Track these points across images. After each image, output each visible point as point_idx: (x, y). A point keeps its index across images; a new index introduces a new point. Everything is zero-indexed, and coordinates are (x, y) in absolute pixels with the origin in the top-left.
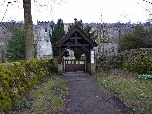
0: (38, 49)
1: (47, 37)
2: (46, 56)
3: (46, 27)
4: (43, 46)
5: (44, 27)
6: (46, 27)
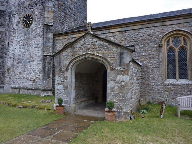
2: (20, 89)
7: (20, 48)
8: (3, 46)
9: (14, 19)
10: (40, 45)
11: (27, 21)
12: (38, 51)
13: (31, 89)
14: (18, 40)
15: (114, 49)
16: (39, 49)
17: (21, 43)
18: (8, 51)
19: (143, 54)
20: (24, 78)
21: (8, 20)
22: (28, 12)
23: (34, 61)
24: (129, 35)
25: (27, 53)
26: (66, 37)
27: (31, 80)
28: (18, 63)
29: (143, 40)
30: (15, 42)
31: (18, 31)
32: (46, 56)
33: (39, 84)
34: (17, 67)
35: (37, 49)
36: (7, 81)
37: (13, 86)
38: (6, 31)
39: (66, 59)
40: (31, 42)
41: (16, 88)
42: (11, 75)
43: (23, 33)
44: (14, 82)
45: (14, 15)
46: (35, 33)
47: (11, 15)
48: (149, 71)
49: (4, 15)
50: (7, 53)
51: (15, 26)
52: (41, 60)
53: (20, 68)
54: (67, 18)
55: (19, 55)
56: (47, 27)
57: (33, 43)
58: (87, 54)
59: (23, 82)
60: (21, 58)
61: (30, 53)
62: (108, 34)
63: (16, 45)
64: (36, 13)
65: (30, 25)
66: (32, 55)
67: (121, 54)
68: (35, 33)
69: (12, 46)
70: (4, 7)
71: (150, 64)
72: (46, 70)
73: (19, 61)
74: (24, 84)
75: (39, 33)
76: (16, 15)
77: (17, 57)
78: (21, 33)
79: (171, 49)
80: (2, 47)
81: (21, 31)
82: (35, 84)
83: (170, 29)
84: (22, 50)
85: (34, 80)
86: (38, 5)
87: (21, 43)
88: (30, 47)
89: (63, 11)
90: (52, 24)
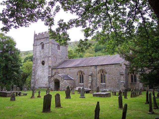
0: (33, 77)
1: (43, 57)
3: (42, 41)
5: (41, 42)
11: (43, 63)
13: (45, 87)
22: (44, 60)
26: (55, 70)
37: (39, 86)
39: (52, 79)
41: (40, 87)
43: (42, 67)
55: (41, 75)
56: (49, 67)
90: (51, 65)
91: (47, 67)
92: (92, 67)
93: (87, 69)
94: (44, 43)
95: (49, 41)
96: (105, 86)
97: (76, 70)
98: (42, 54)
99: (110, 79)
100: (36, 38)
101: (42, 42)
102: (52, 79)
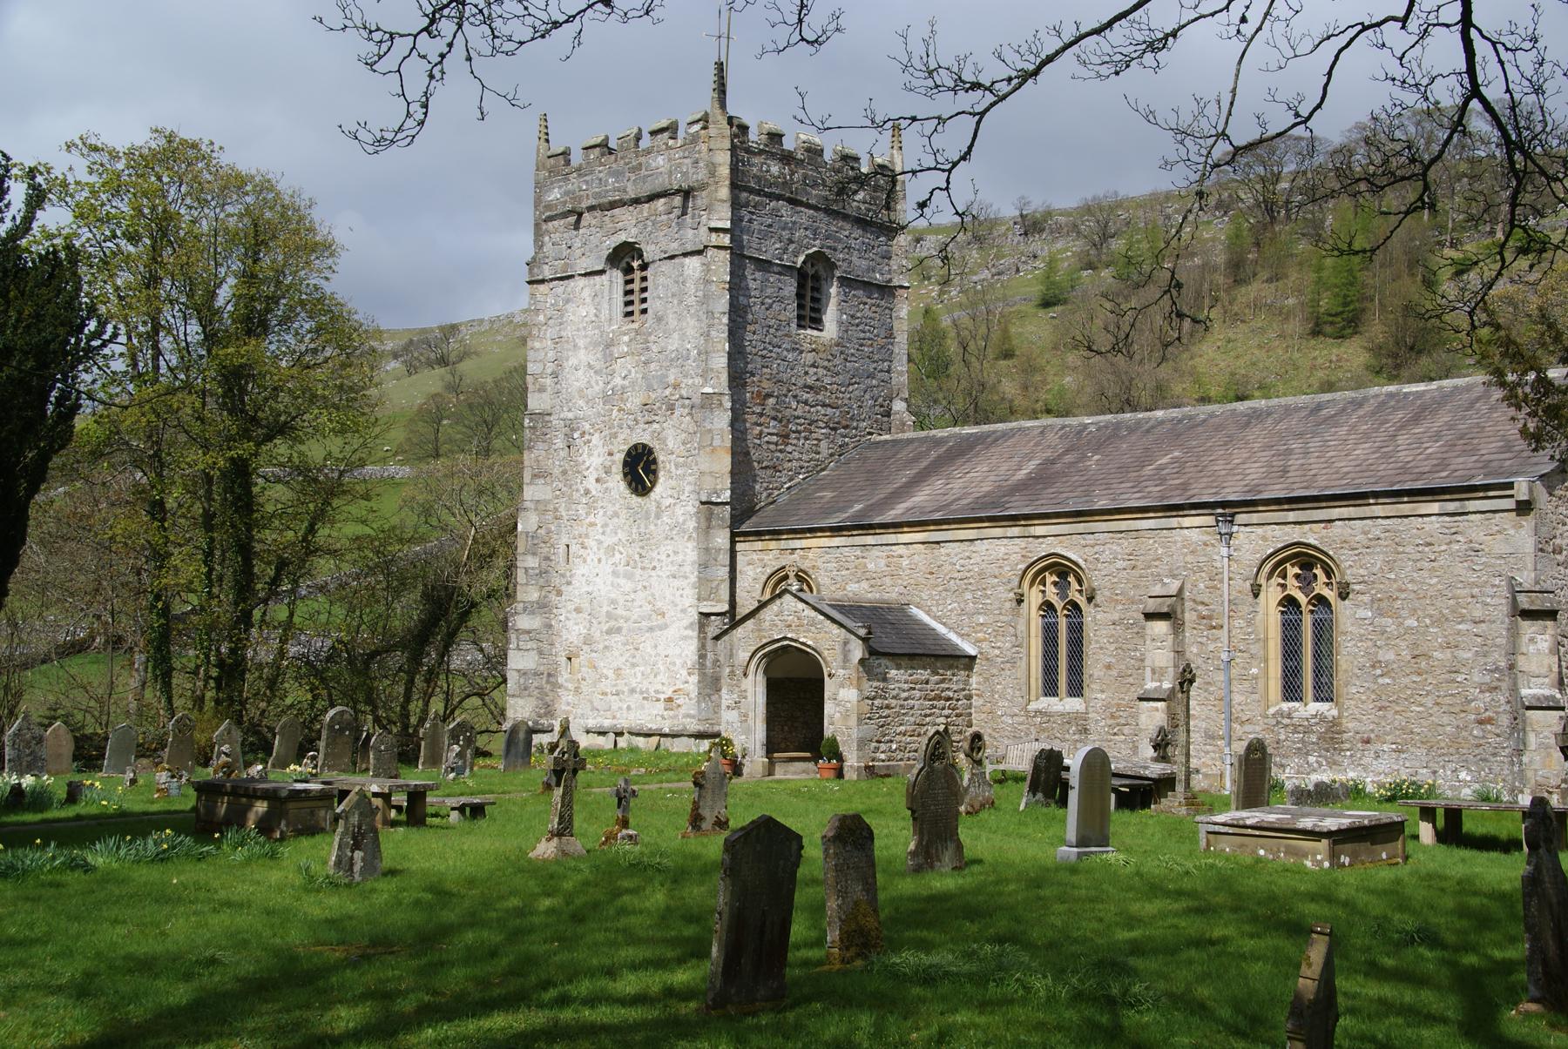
1: (634, 401)
2: (619, 734)
3: (627, 226)
4: (591, 557)
6: (627, 226)
7: (615, 574)
8: (547, 559)
9: (590, 455)
10: (687, 569)
12: (681, 592)
14: (609, 540)
15: (835, 630)
16: (684, 583)
17: (617, 555)
18: (569, 583)
19: (981, 621)
20: (633, 691)
21: (562, 454)
22: (645, 439)
23: (666, 626)
24: (948, 555)
25: (641, 595)
26: (773, 545)
27: (658, 700)
28: (609, 632)
29: (981, 574)
30: (595, 549)
31: (604, 504)
32: (708, 615)
33: (688, 716)
34: (606, 647)
35: (676, 583)
36: (568, 704)
38: (557, 497)
40: (654, 554)
42: (584, 679)
43: (623, 514)
44: (594, 709)
45: (587, 437)
46: (669, 521)
47: (576, 436)
48: (995, 671)
49: (548, 431)
50: (563, 588)
51: (591, 483)
52: (690, 626)
53: (616, 653)
54: (793, 435)
55: (613, 602)
57: (663, 557)
58: (785, 638)
59: (629, 708)
60: (620, 612)
61: (653, 595)
62: (894, 548)
63: (599, 561)
64: (671, 445)
65: (651, 489)
66: (659, 604)
67: (846, 643)
68: (669, 521)
69: (585, 561)
70: (544, 395)
71: (997, 652)
72: (708, 664)
73: (612, 623)
74: (632, 716)
75: (684, 521)
76: (596, 439)
77: (605, 609)
78: (616, 514)
79: (1048, 607)
80: (544, 564)
81: (617, 506)
82: (671, 713)
83: (1043, 548)
84: (622, 581)
85: (670, 700)
86: (677, 413)
87: (617, 555)
88: (653, 573)
89: (774, 418)
91: (685, 512)
92: (1187, 522)
93: (1127, 544)
94: (650, 252)
95: (703, 230)
96: (1331, 738)
97: (1000, 549)
98: (626, 369)
99: (1388, 655)
100: (555, 195)
101: (622, 237)
102: (745, 641)
